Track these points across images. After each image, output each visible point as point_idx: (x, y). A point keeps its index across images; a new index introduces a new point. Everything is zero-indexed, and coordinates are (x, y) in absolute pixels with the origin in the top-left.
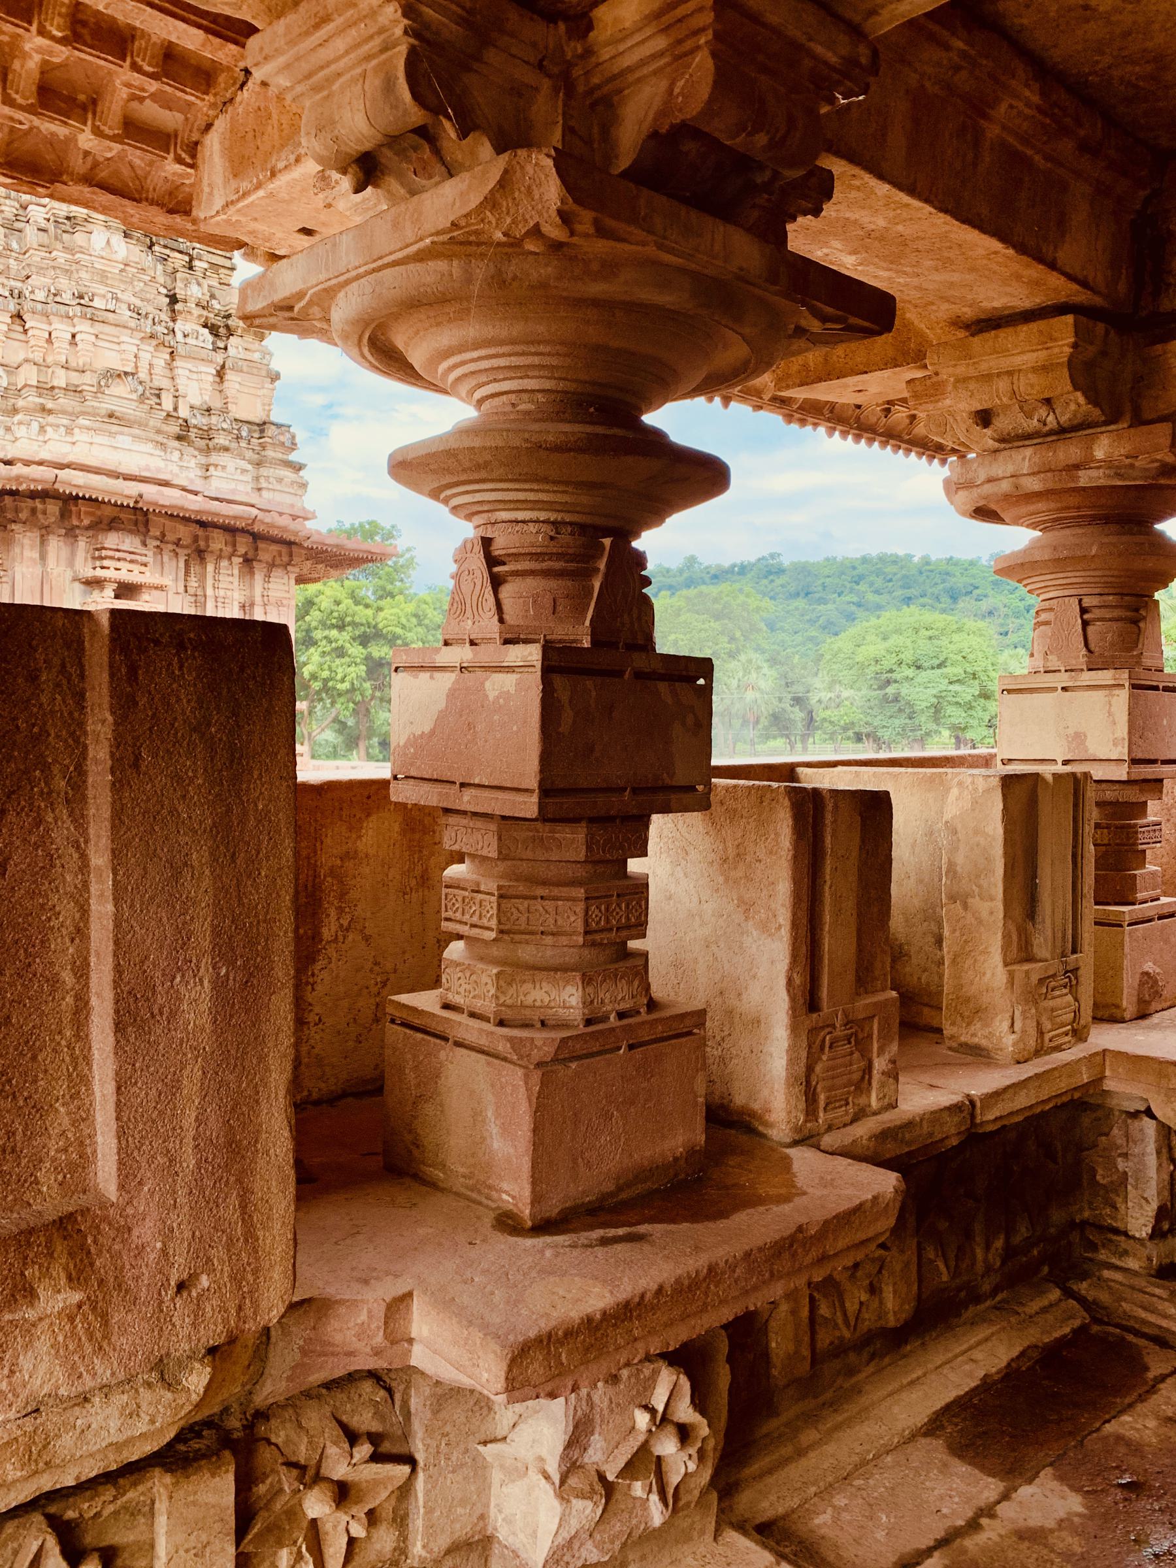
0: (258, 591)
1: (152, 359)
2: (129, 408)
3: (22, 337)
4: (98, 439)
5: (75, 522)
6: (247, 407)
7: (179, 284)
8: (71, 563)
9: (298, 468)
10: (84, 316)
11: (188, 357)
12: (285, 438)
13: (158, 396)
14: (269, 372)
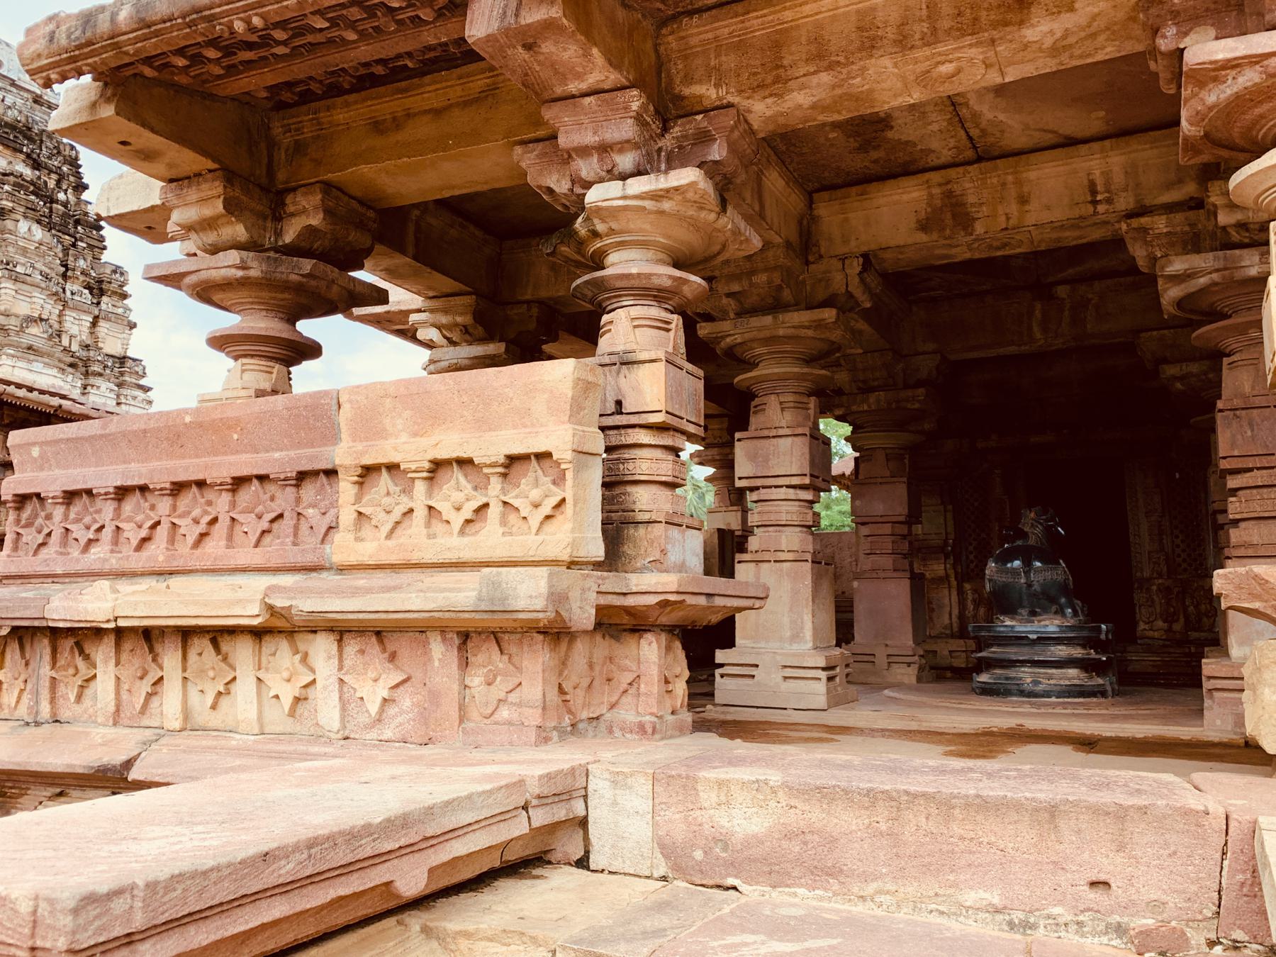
1: (51, 309)
2: (39, 343)
4: (20, 364)
6: (111, 345)
7: (71, 258)
9: (146, 389)
10: (10, 278)
11: (75, 309)
12: (139, 369)
13: (59, 336)
14: (129, 322)
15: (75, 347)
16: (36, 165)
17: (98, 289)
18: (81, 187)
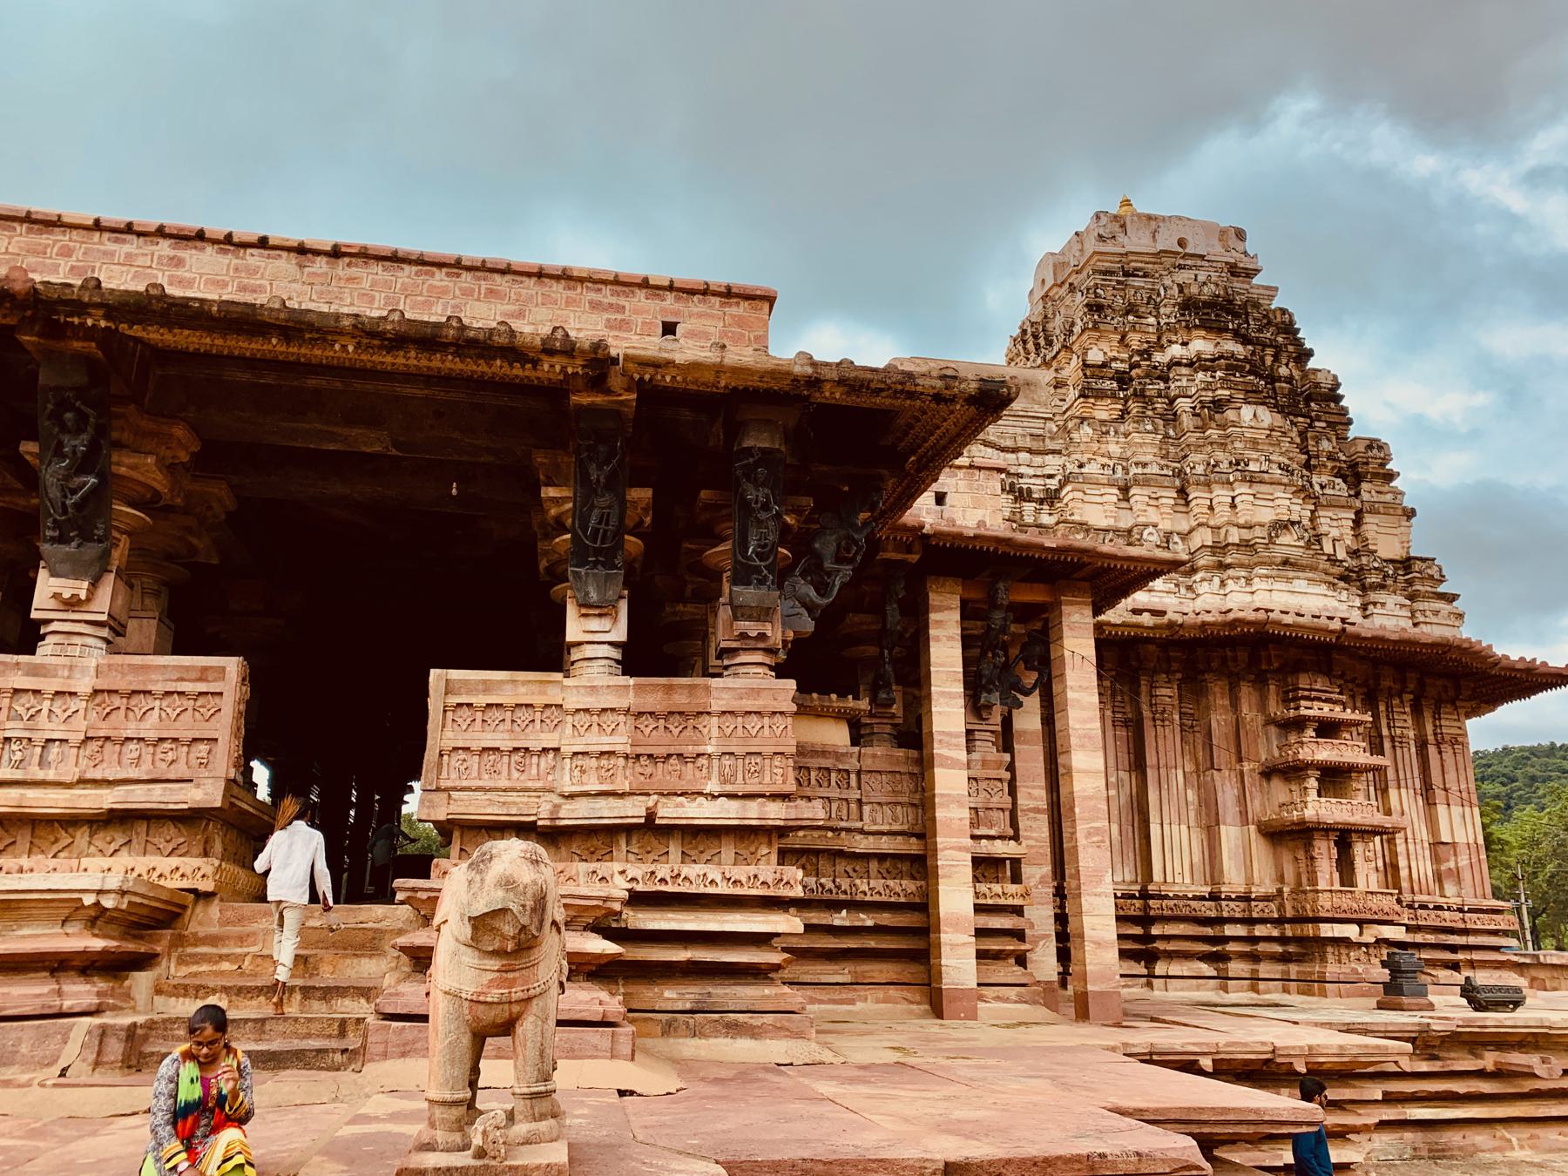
0: (1429, 728)
1: (1299, 510)
2: (1296, 554)
3: (1183, 509)
4: (1277, 586)
5: (1264, 667)
6: (1387, 546)
7: (1311, 442)
8: (1262, 707)
9: (1450, 598)
10: (1244, 480)
11: (1330, 506)
12: (1433, 571)
13: (1319, 542)
14: (1404, 509)
15: (1341, 555)
16: (1245, 340)
17: (1353, 474)
18: (1304, 355)
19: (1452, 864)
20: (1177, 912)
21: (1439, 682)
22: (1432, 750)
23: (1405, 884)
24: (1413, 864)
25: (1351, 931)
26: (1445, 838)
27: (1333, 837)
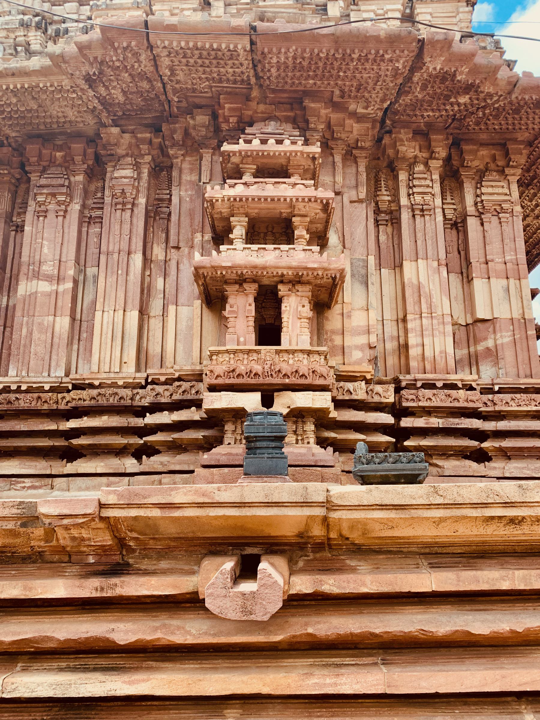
0: (469, 199)
19: (490, 343)
20: (102, 401)
21: (484, 152)
22: (472, 223)
23: (413, 364)
24: (427, 341)
25: (251, 401)
26: (481, 314)
27: (252, 289)
